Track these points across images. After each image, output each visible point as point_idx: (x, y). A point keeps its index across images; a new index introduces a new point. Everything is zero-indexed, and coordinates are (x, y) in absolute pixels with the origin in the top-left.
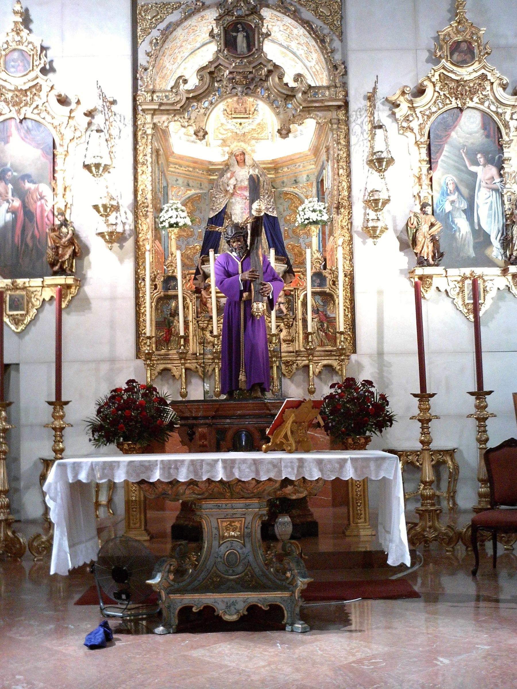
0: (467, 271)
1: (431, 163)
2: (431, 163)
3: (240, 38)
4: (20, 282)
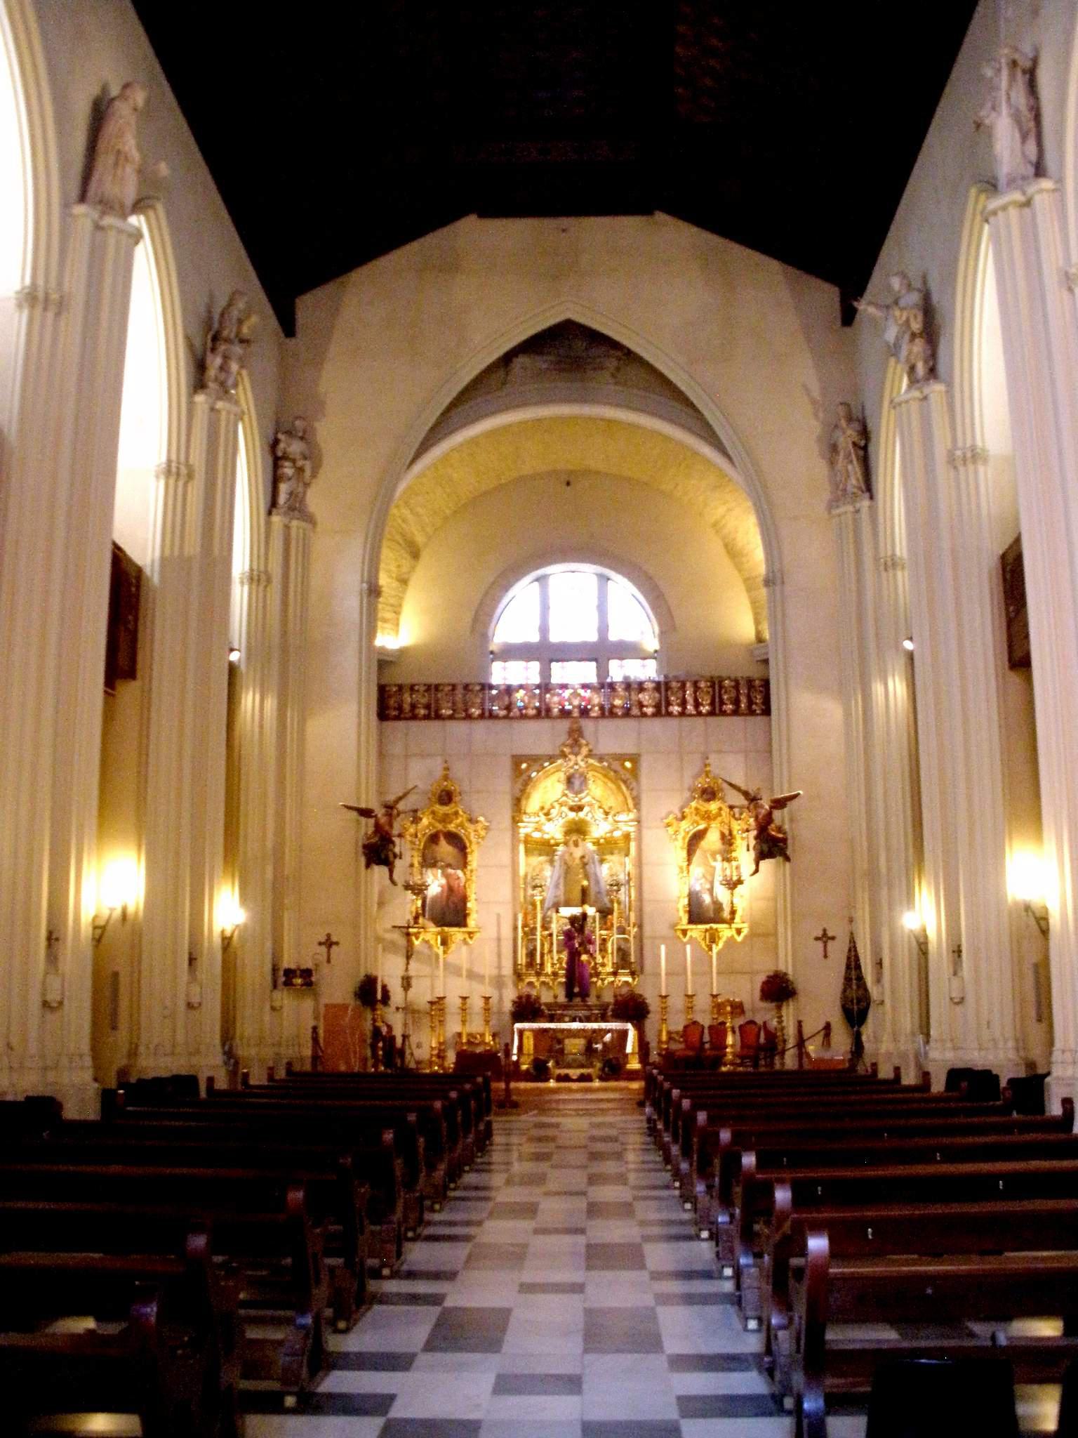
0: (708, 926)
1: (689, 860)
2: (689, 860)
3: (577, 783)
4: (446, 929)
